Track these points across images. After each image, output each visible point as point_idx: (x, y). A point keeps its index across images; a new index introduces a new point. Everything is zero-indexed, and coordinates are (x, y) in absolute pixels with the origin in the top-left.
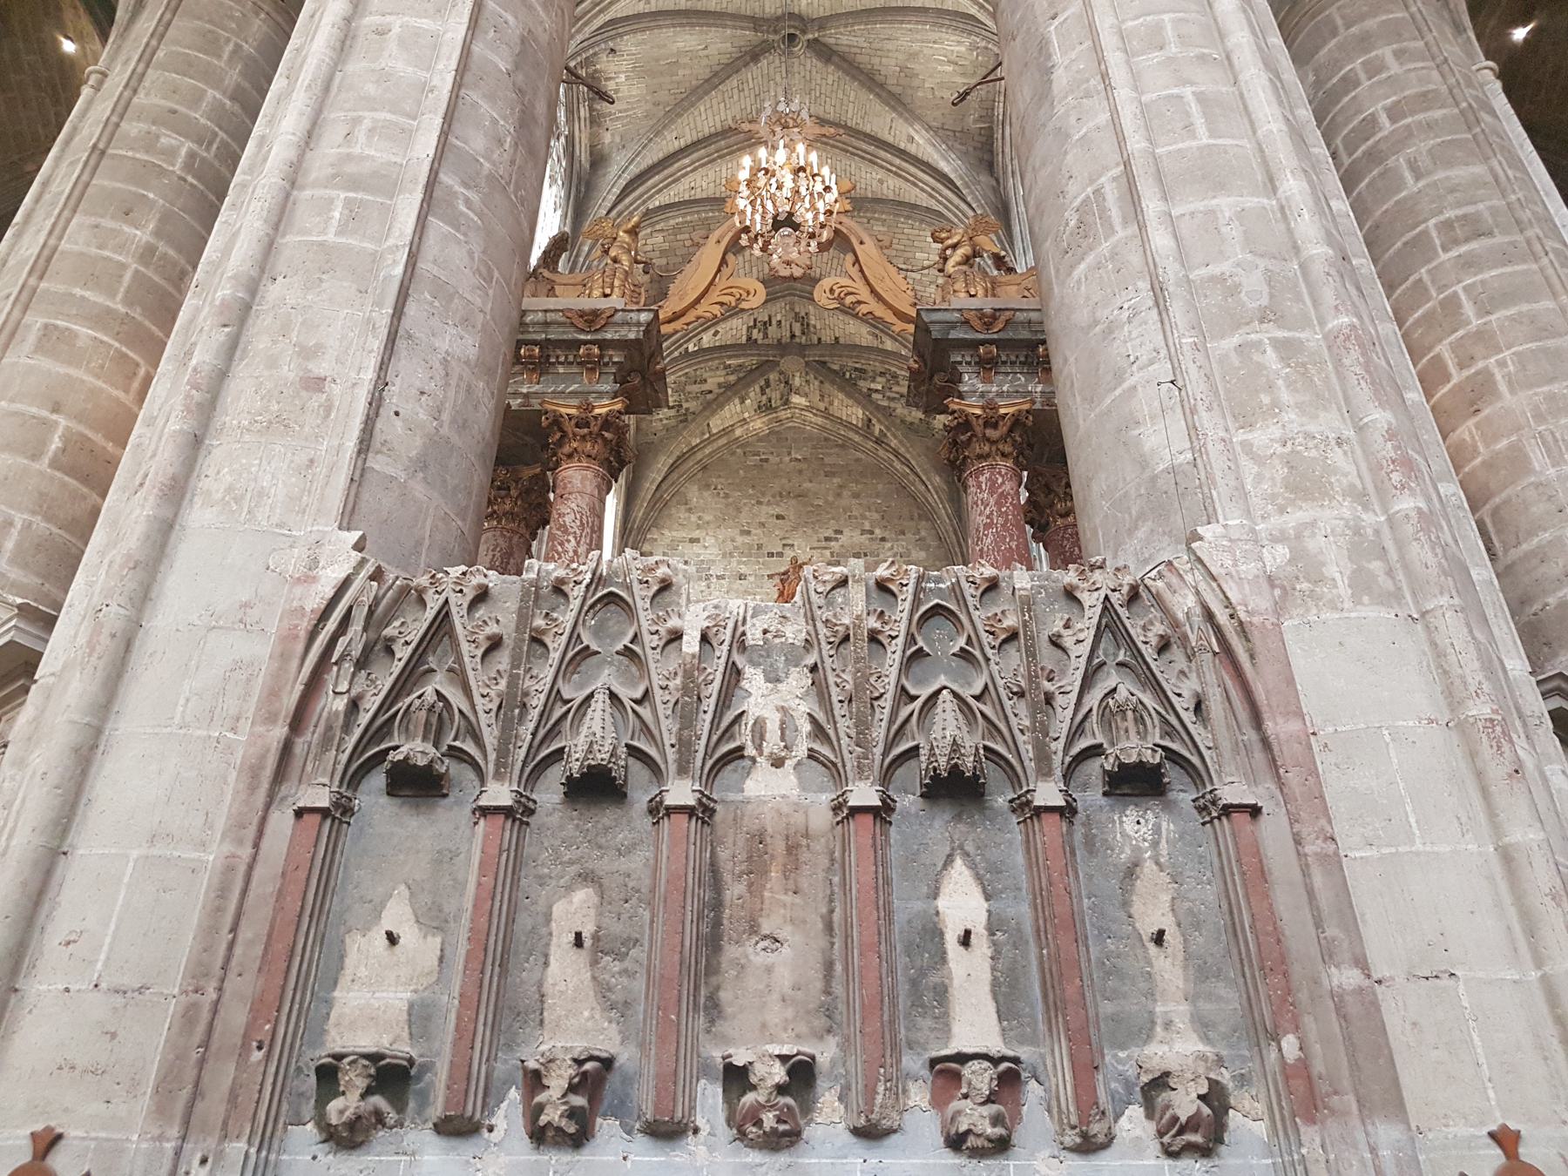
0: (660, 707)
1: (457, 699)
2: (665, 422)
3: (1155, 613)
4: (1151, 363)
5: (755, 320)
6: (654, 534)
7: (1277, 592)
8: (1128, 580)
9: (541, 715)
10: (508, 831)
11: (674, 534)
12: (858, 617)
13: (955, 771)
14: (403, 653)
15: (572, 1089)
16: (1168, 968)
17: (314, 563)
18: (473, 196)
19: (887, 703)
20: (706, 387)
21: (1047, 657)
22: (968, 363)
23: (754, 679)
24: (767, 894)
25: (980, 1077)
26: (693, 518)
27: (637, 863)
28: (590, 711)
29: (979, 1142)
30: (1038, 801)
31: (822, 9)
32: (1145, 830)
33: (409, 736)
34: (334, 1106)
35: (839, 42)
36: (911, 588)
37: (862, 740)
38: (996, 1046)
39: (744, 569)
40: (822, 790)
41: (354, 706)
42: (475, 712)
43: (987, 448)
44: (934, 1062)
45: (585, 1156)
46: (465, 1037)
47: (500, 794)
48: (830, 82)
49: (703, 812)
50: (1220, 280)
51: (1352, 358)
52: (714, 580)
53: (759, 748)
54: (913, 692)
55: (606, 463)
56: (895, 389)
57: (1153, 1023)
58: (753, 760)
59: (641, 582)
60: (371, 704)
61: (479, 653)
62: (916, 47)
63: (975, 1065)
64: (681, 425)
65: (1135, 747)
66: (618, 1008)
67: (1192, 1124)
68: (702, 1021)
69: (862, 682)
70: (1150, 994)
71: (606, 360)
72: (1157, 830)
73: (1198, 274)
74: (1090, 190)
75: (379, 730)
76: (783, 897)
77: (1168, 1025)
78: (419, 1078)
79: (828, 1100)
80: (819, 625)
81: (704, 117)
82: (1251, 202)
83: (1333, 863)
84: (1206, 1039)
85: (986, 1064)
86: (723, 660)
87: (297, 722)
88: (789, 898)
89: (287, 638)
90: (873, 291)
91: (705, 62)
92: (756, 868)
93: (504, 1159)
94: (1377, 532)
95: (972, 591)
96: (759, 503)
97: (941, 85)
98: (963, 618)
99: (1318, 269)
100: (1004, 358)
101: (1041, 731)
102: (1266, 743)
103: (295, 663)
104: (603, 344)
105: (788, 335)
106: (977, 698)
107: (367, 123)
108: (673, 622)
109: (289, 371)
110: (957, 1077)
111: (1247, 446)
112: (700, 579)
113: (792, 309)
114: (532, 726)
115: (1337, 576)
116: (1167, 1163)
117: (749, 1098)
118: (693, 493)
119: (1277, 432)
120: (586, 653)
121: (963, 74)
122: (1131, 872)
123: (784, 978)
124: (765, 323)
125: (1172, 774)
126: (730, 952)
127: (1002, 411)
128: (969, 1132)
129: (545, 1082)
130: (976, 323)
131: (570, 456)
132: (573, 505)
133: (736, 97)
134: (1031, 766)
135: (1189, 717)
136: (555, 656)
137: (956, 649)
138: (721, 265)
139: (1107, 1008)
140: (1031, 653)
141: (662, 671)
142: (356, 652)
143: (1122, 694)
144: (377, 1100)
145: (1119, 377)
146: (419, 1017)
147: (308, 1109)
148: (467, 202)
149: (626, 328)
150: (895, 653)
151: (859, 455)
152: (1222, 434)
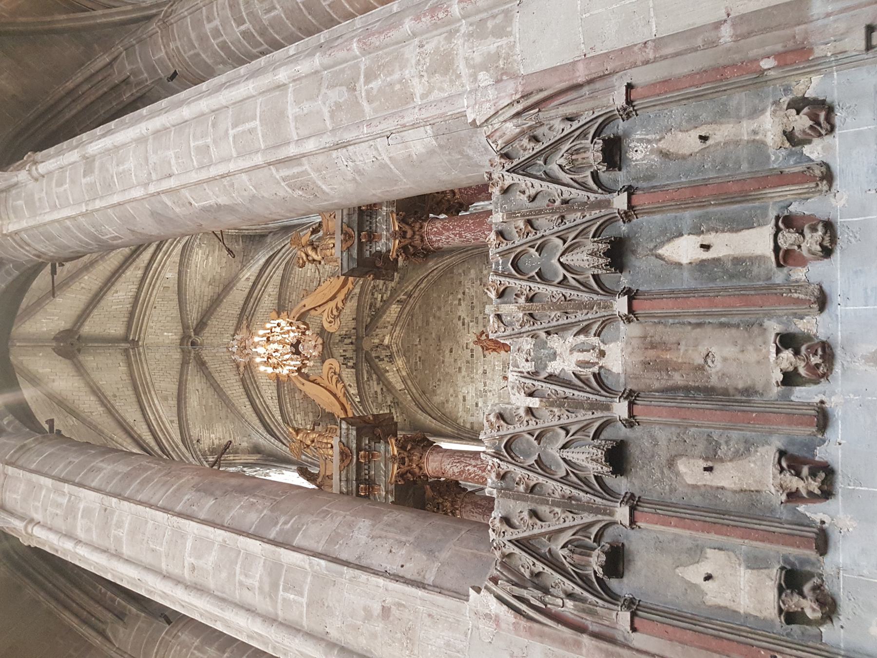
0: (571, 420)
1: (566, 537)
2: (398, 414)
3: (516, 144)
4: (377, 149)
6: (461, 421)
7: (505, 78)
8: (497, 159)
9: (576, 488)
10: (644, 508)
11: (460, 410)
12: (519, 308)
13: (607, 254)
14: (540, 567)
15: (798, 474)
16: (721, 133)
17: (487, 616)
18: (282, 520)
19: (568, 292)
20: (379, 391)
21: (541, 203)
22: (371, 247)
23: (554, 367)
24: (680, 360)
25: (788, 239)
26: (452, 399)
27: (662, 435)
28: (573, 460)
29: (827, 238)
30: (625, 207)
31: (178, 328)
32: (641, 147)
33: (588, 564)
34: (810, 614)
36: (502, 279)
37: (590, 306)
38: (768, 230)
39: (481, 371)
40: (618, 329)
41: (570, 596)
42: (574, 526)
43: (417, 237)
44: (779, 265)
45: (839, 467)
46: (768, 537)
47: (622, 513)
49: (632, 397)
50: (332, 114)
51: (375, 41)
52: (486, 388)
53: (594, 364)
54: (561, 278)
55: (424, 448)
56: (381, 287)
57: (754, 141)
58: (601, 367)
59: (498, 430)
60: (569, 586)
61: (539, 523)
62: (199, 277)
63: (781, 242)
64: (400, 406)
65: (593, 154)
66: (747, 448)
67: (814, 118)
68: (756, 398)
69: (556, 306)
70: (737, 143)
71: (367, 447)
72: (641, 141)
73: (329, 125)
74: (283, 184)
75: (585, 582)
76: (682, 351)
77: (755, 132)
78: (793, 564)
79: (802, 326)
80: (523, 330)
81: (234, 392)
82: (290, 97)
83: (659, 42)
84: (763, 111)
85: (780, 235)
86: (544, 384)
87: (580, 629)
88: (682, 348)
89: (531, 633)
90: (331, 299)
91: (205, 391)
92: (664, 367)
93: (841, 515)
94: (471, 25)
95: (504, 245)
96: (443, 362)
97: (219, 263)
98: (519, 250)
99: (327, 60)
100: (368, 228)
101: (584, 206)
102: (590, 82)
103: (546, 629)
104: (359, 449)
105: (351, 346)
106: (565, 242)
107: (243, 578)
108: (522, 412)
109: (379, 627)
110: (787, 252)
111: (423, 96)
112: (486, 396)
113: (337, 344)
114: (582, 494)
115: (496, 45)
116: (837, 131)
117: (802, 371)
118: (438, 399)
119: (416, 81)
120: (539, 462)
121: (214, 252)
122: (665, 155)
123: (730, 351)
125: (608, 133)
126: (714, 381)
127: (397, 228)
128: (821, 245)
129: (794, 490)
130: (349, 243)
131: (421, 468)
132: (448, 467)
133: (224, 374)
134: (604, 212)
135: (576, 125)
136: (541, 479)
137: (537, 254)
138: (316, 383)
139: (745, 167)
140: (540, 212)
141: (549, 419)
142: (539, 594)
143: (562, 161)
144: (807, 588)
145: (383, 166)
146: (755, 563)
147: (811, 630)
148: (285, 523)
149: (350, 436)
150: (539, 288)
151: (417, 307)
152: (417, 110)
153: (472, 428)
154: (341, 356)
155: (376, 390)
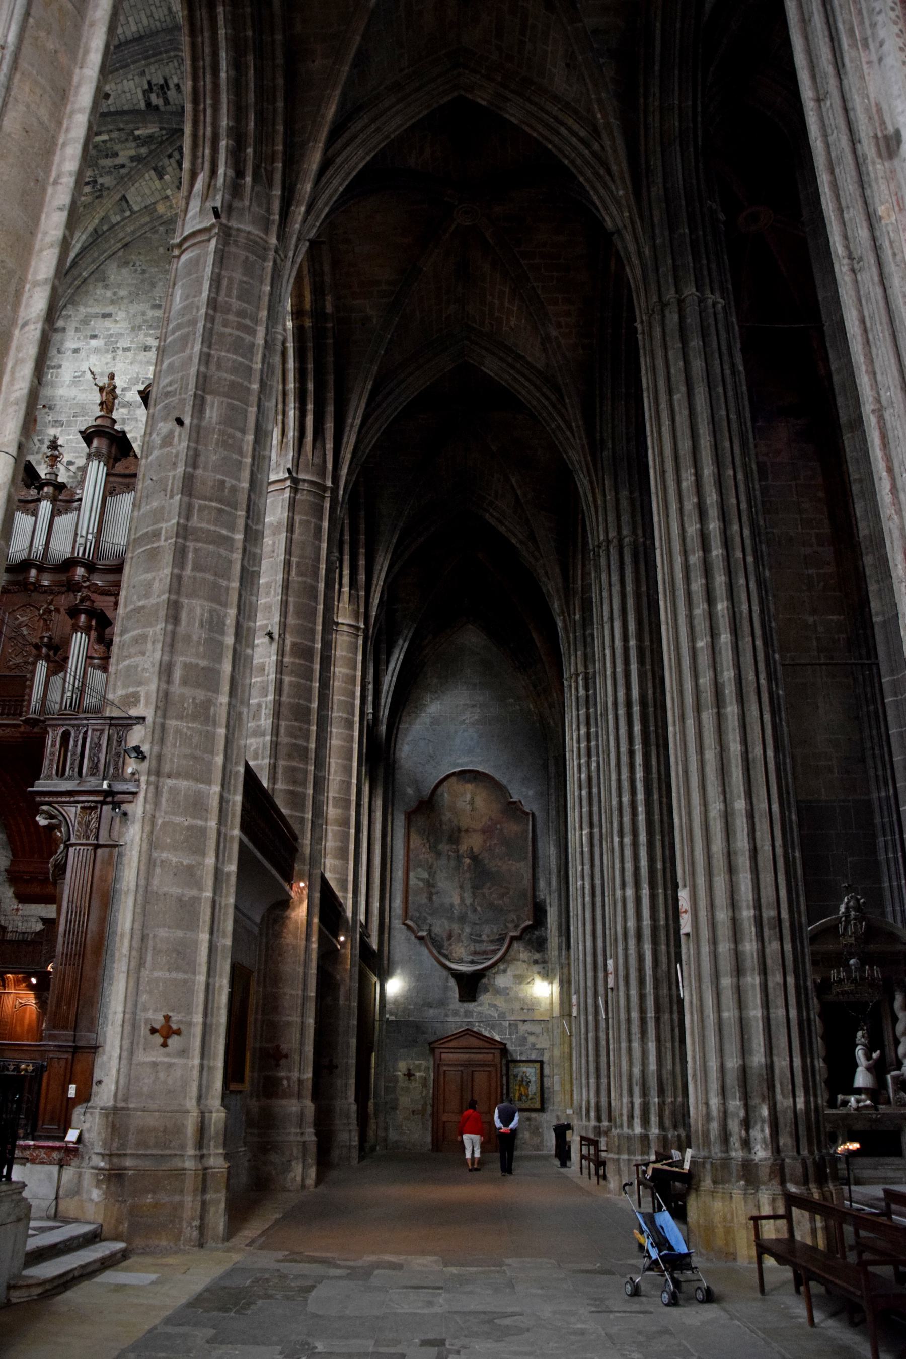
5: (149, 82)
6: (70, 311)
11: (89, 309)
20: (119, 161)
26: (109, 294)
64: (97, 201)
112: (107, 351)
124: (162, 87)
153: (56, 330)
155: (121, 153)
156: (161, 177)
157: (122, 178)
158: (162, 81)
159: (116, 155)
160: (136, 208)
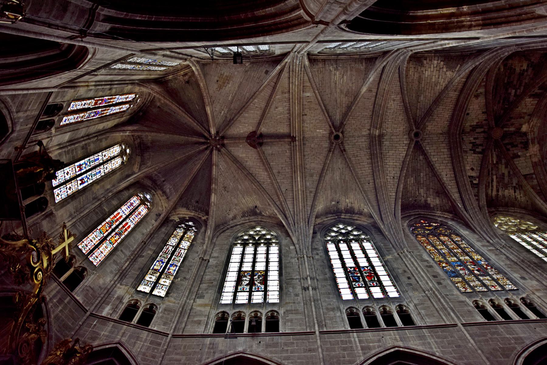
2: (522, 195)
5: (470, 150)
31: (326, 126)
35: (339, 119)
48: (355, 122)
56: (515, 82)
62: (338, 91)
64: (523, 188)
81: (364, 172)
91: (344, 170)
97: (351, 80)
113: (468, 133)
121: (347, 71)
133: (359, 158)
154: (470, 143)
155: (503, 172)
156: (519, 157)
157: (514, 173)
158: (471, 145)
159: (503, 174)
160: (532, 171)
